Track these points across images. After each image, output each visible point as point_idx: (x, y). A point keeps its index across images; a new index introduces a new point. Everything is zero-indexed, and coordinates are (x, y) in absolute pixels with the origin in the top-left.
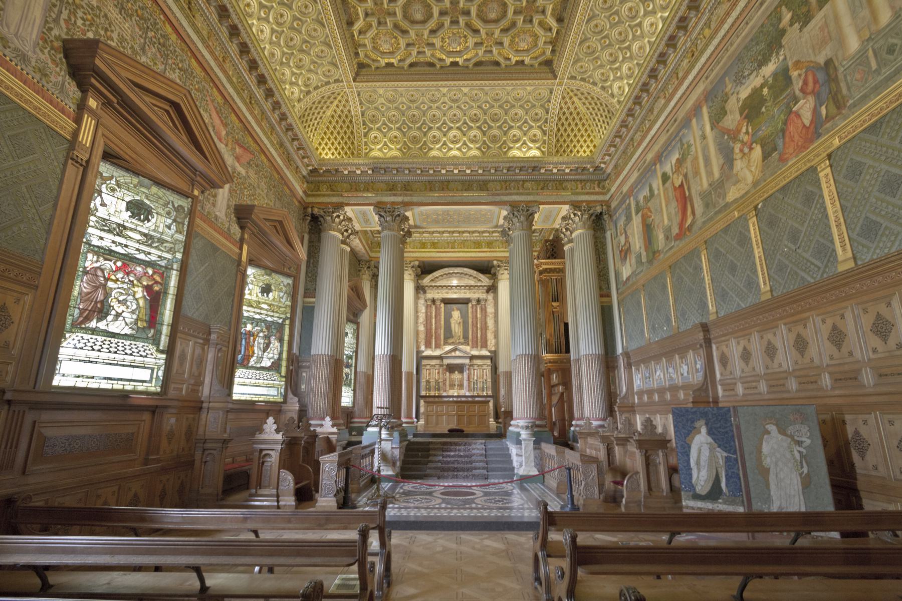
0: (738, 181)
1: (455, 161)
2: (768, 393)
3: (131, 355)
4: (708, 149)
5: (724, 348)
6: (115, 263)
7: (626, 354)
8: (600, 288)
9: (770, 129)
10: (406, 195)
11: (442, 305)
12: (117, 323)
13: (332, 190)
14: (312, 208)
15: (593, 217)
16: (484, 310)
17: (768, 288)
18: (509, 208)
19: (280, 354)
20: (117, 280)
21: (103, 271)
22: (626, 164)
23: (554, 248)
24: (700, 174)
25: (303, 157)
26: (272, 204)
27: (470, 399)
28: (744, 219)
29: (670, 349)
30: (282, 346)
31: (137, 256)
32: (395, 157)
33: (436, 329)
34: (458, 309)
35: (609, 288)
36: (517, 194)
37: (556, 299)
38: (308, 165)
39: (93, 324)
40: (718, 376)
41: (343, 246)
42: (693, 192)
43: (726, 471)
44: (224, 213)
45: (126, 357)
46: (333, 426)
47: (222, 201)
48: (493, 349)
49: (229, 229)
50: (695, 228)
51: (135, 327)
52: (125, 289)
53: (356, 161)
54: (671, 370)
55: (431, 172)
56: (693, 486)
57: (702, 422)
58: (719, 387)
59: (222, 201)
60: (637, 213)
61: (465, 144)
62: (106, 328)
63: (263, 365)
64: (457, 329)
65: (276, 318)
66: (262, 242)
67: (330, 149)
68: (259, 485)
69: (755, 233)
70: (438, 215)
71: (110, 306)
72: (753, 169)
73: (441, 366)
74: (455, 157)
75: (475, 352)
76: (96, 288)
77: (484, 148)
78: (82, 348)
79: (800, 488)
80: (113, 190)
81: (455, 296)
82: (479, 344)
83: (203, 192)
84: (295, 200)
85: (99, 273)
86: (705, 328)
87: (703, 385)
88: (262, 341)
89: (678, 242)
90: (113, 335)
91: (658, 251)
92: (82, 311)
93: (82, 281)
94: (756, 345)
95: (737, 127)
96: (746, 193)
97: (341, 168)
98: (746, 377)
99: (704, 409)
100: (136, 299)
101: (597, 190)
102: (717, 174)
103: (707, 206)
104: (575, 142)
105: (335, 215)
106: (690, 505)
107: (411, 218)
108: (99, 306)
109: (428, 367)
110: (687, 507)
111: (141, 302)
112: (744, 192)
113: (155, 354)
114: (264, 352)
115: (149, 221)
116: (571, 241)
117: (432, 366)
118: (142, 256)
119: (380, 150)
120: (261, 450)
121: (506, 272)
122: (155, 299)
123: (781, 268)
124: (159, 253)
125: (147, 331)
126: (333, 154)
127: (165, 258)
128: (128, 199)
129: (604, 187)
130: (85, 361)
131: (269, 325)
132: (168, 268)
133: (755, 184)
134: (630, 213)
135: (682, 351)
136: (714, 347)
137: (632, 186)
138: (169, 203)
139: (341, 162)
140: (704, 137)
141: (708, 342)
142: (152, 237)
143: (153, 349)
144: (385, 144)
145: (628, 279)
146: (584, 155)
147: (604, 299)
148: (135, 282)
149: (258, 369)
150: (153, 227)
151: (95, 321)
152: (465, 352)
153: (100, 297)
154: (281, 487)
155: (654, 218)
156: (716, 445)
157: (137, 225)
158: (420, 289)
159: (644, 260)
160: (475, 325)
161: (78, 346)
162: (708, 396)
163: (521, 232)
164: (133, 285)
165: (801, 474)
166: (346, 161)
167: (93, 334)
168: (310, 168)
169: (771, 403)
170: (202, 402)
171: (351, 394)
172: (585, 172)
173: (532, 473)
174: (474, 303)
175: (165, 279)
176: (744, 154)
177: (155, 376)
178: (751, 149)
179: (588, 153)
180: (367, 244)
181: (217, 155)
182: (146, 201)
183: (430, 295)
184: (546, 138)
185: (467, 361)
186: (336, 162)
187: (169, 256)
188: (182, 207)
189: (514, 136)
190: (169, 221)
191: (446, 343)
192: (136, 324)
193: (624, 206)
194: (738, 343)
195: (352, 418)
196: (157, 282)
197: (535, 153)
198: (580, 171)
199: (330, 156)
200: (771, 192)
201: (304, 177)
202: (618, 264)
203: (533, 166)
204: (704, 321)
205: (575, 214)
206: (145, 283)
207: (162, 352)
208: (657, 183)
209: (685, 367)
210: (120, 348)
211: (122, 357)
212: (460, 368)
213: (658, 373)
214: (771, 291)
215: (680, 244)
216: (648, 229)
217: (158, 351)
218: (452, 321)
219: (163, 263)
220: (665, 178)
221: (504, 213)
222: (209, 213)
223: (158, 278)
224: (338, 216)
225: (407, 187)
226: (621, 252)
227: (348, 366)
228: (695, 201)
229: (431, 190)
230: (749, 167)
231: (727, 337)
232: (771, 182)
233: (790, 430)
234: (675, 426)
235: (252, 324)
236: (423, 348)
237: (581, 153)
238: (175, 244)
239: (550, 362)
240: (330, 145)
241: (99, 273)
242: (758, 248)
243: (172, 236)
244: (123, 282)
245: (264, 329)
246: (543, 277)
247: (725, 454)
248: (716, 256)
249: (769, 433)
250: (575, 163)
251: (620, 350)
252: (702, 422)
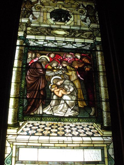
3: (78, 136)
6: (49, 56)
12: (61, 106)
20: (53, 68)
21: (40, 64)
45: (74, 138)
52: (60, 76)
71: (51, 92)
76: (37, 79)
78: (33, 135)
80: (40, 8)
85: (38, 66)
90: (60, 119)
92: (29, 100)
93: (26, 75)
100: (72, 82)
108: (42, 93)
111: (77, 84)
113: (101, 131)
115: (68, 20)
118: (69, 46)
124: (82, 41)
127: (88, 44)
128: (51, 11)
130: (37, 147)
138: (80, 6)
142: (73, 31)
148: (68, 67)
151: (41, 108)
153: (42, 86)
157: (60, 25)
161: (30, 132)
164: (67, 70)
177: (106, 155)
187: (91, 41)
188: (91, 6)
190: (84, 17)
192: (77, 105)
196: (86, 64)
206: (76, 67)
207: (106, 129)
210: (67, 131)
211: (70, 139)
217: (103, 128)
219: (87, 48)
223: (86, 61)
238: (93, 31)
241: (38, 66)
243: (89, 26)
244: (58, 70)
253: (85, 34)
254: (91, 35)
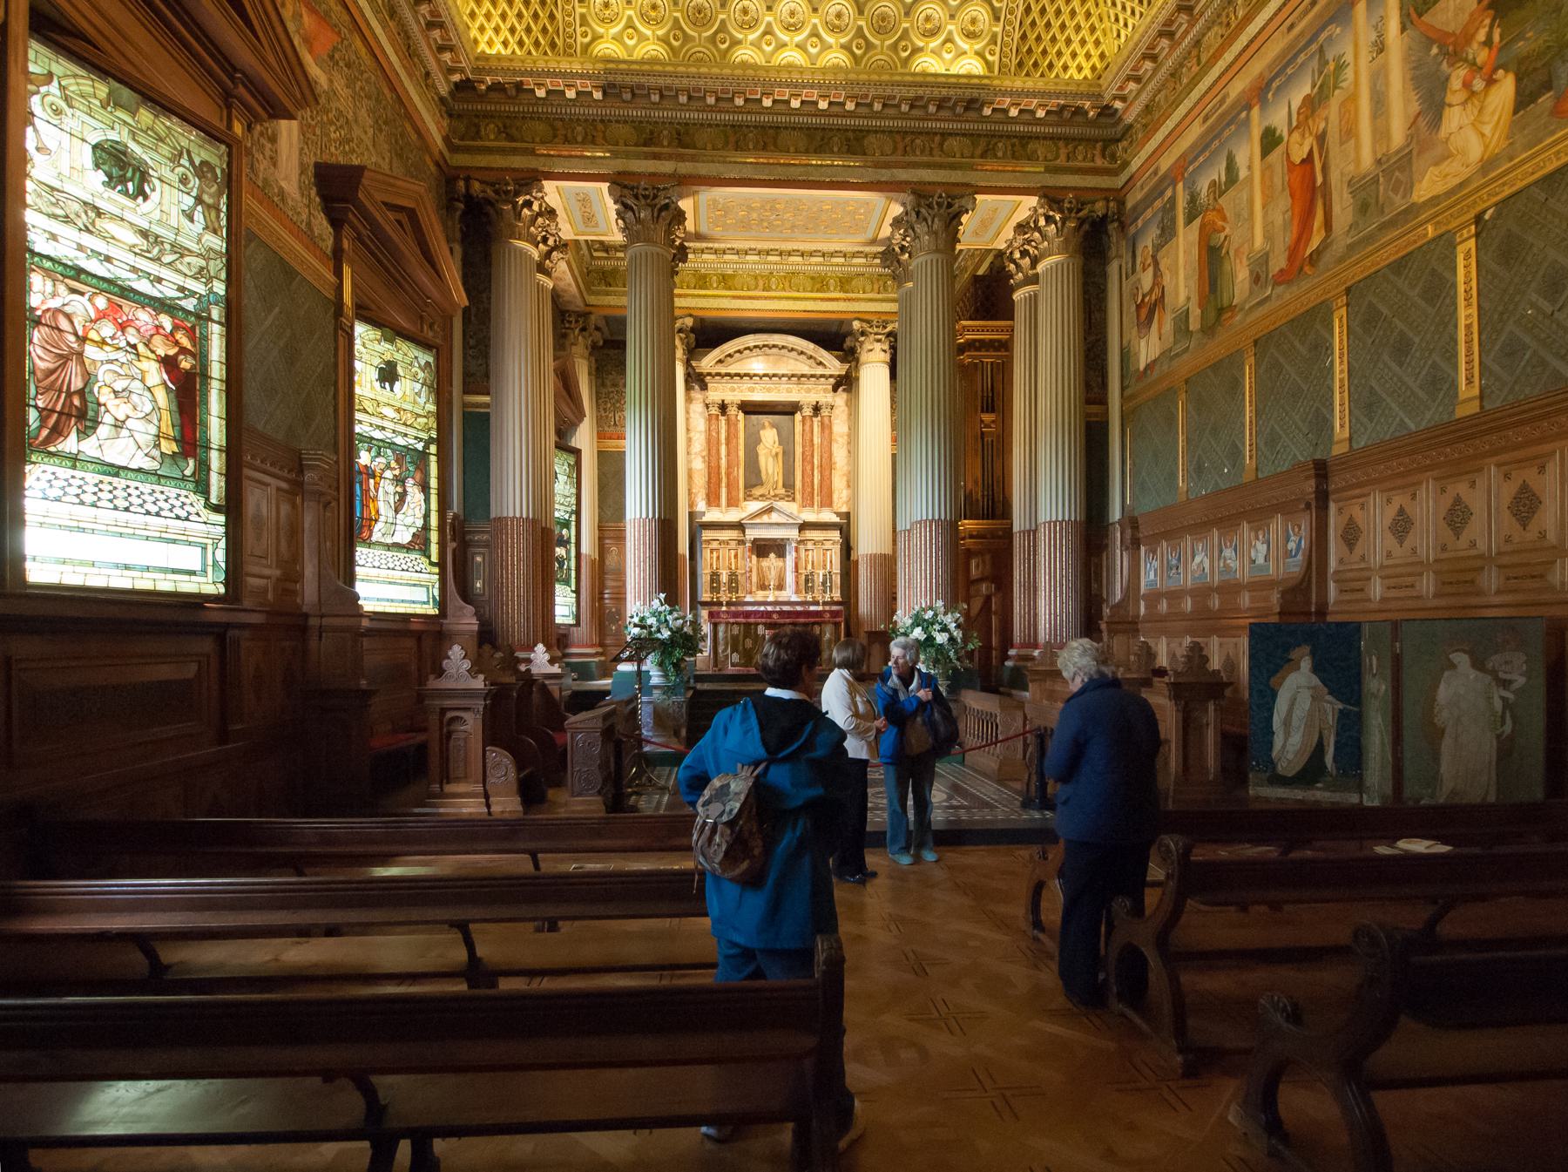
0: (1447, 156)
1: (795, 76)
2: (1436, 596)
3: (158, 514)
4: (1387, 76)
5: (1356, 511)
7: (1131, 522)
8: (1088, 386)
9: (1545, 36)
10: (681, 158)
11: (741, 415)
13: (511, 138)
14: (467, 180)
15: (1086, 227)
16: (826, 428)
17: (1476, 392)
18: (909, 198)
19: (427, 516)
20: (104, 342)
22: (1176, 104)
23: (989, 293)
24: (1357, 137)
25: (441, 49)
26: (385, 166)
27: (799, 608)
28: (1446, 243)
29: (1228, 512)
30: (427, 500)
31: (135, 285)
32: (654, 61)
33: (729, 467)
34: (773, 426)
35: (1104, 385)
36: (928, 166)
37: (989, 408)
38: (451, 71)
39: (70, 444)
40: (1333, 564)
41: (539, 276)
42: (1335, 176)
43: (1338, 734)
44: (296, 185)
46: (552, 661)
47: (288, 151)
48: (844, 509)
49: (309, 224)
50: (1327, 258)
51: (156, 453)
53: (564, 65)
54: (1228, 553)
55: (739, 102)
56: (1272, 762)
57: (1306, 649)
58: (1332, 586)
59: (288, 151)
60: (1190, 219)
61: (815, 34)
62: (96, 454)
63: (397, 539)
64: (770, 467)
65: (410, 439)
66: (382, 258)
67: (497, 30)
68: (446, 777)
69: (1467, 274)
70: (750, 209)
72: (1487, 130)
73: (741, 542)
74: (790, 67)
75: (810, 516)
76: (64, 359)
77: (859, 46)
78: (58, 500)
79: (1494, 758)
82: (817, 499)
83: (249, 128)
84: (427, 158)
86: (1321, 470)
87: (1303, 580)
88: (391, 489)
89: (1279, 289)
90: (116, 470)
91: (1231, 308)
94: (1427, 505)
95: (1466, 27)
96: (1461, 185)
97: (530, 82)
98: (1396, 566)
99: (1302, 626)
101: (1099, 162)
102: (1398, 137)
103: (1363, 209)
104: (1061, 44)
105: (521, 200)
106: (1261, 792)
107: (689, 215)
108: (77, 402)
109: (715, 545)
110: (1258, 798)
111: (161, 395)
112: (1457, 181)
114: (397, 511)
116: (1034, 280)
119: (617, 38)
120: (443, 711)
121: (878, 346)
122: (186, 391)
123: (1512, 351)
124: (180, 280)
125: (182, 464)
126: (505, 44)
129: (1113, 157)
130: (70, 529)
131: (402, 454)
132: (202, 317)
133: (1487, 165)
134: (1173, 220)
135: (1258, 515)
136: (1333, 507)
137: (1183, 156)
138: (181, 155)
139: (529, 66)
140: (1380, 47)
141: (1322, 498)
143: (197, 501)
144: (630, 25)
145: (1149, 367)
146: (1077, 76)
147: (1094, 409)
148: (141, 348)
149: (389, 547)
150: (156, 215)
151: (73, 435)
153: (77, 384)
154: (491, 780)
155: (1232, 234)
156: (1326, 690)
159: (1194, 324)
160: (807, 459)
162: (1309, 602)
163: (934, 257)
165: (1498, 737)
166: (541, 65)
167: (74, 467)
168: (456, 78)
169: (1440, 614)
170: (306, 616)
171: (572, 598)
172: (1079, 119)
174: (808, 412)
175: (201, 342)
176: (1473, 93)
177: (210, 562)
178: (1491, 82)
179: (1087, 72)
180: (581, 273)
181: (279, 29)
182: (132, 145)
183: (719, 392)
184: (998, 29)
185: (793, 534)
186: (517, 65)
187: (199, 288)
189: (928, 19)
191: (748, 497)
192: (157, 446)
193: (1158, 204)
194: (1389, 501)
195: (566, 646)
196: (183, 350)
197: (970, 66)
198: (1067, 115)
199: (498, 48)
200: (1519, 185)
201: (442, 100)
202: (1132, 333)
203: (963, 100)
204: (1318, 456)
205: (1049, 219)
207: (216, 509)
208: (1247, 153)
209: (1262, 548)
212: (778, 547)
213: (1198, 559)
214: (1482, 397)
215: (1287, 293)
216: (1212, 258)
218: (762, 451)
219: (190, 304)
220: (1270, 141)
221: (896, 210)
222: (265, 180)
223: (185, 342)
224: (528, 204)
225: (684, 138)
226: (1138, 307)
227: (564, 543)
228: (1335, 197)
229: (737, 148)
230: (1479, 125)
231: (1365, 490)
232: (1523, 162)
233: (1494, 661)
234: (1251, 657)
235: (369, 450)
237: (1072, 71)
238: (207, 259)
239: (971, 537)
240: (497, 19)
241: (64, 324)
242: (1468, 305)
245: (393, 464)
246: (966, 358)
247: (1341, 706)
248: (1366, 322)
249: (1452, 666)
250: (1058, 95)
251: (1116, 514)
252: (1306, 649)
253: (187, 259)
254: (202, 269)
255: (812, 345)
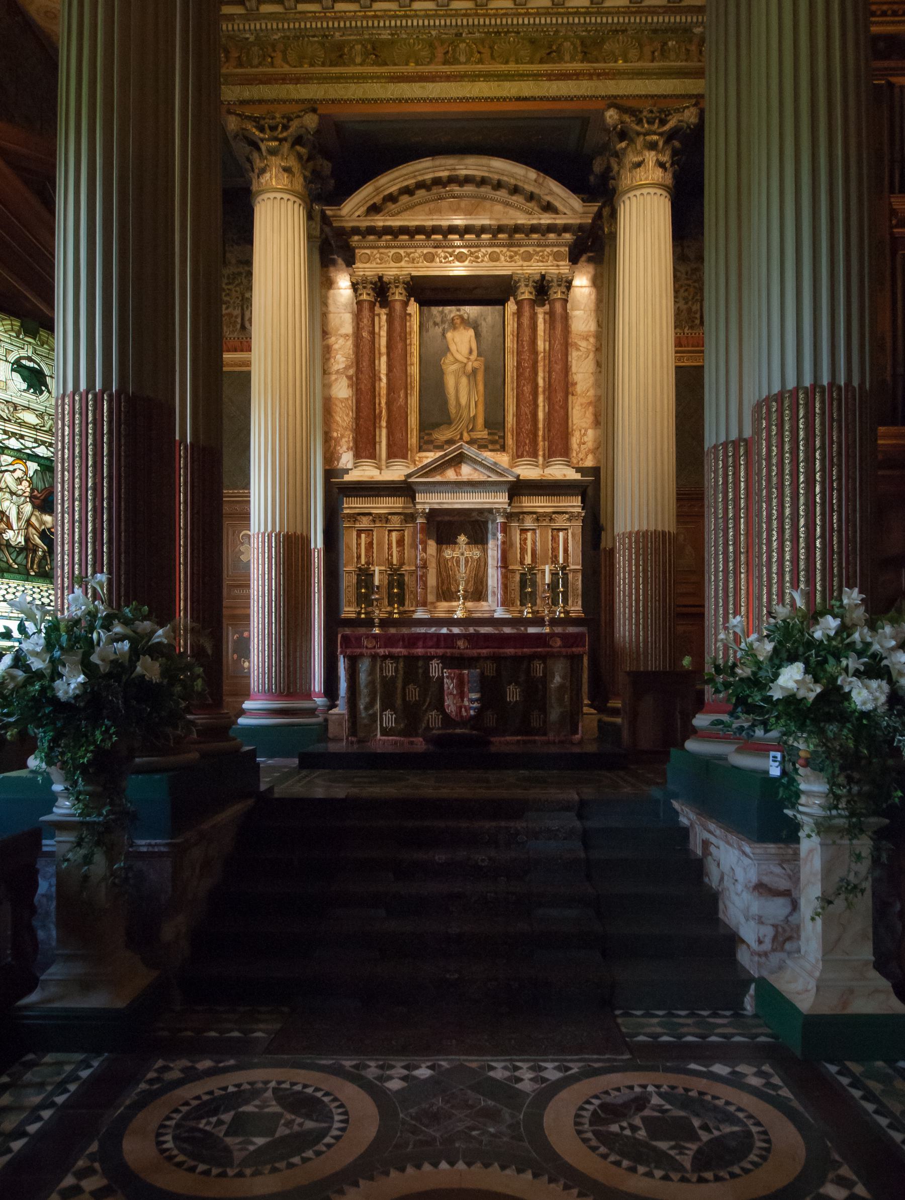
11: (413, 308)
16: (560, 322)
27: (507, 630)
48: (589, 462)
73: (409, 518)
75: (528, 472)
81: (459, 270)
109: (365, 523)
117: (376, 518)
121: (651, 157)
152: (492, 469)
158: (330, 247)
173: (862, 1006)
174: (526, 293)
185: (500, 500)
212: (474, 525)
236: (346, 459)
255: (532, 174)
